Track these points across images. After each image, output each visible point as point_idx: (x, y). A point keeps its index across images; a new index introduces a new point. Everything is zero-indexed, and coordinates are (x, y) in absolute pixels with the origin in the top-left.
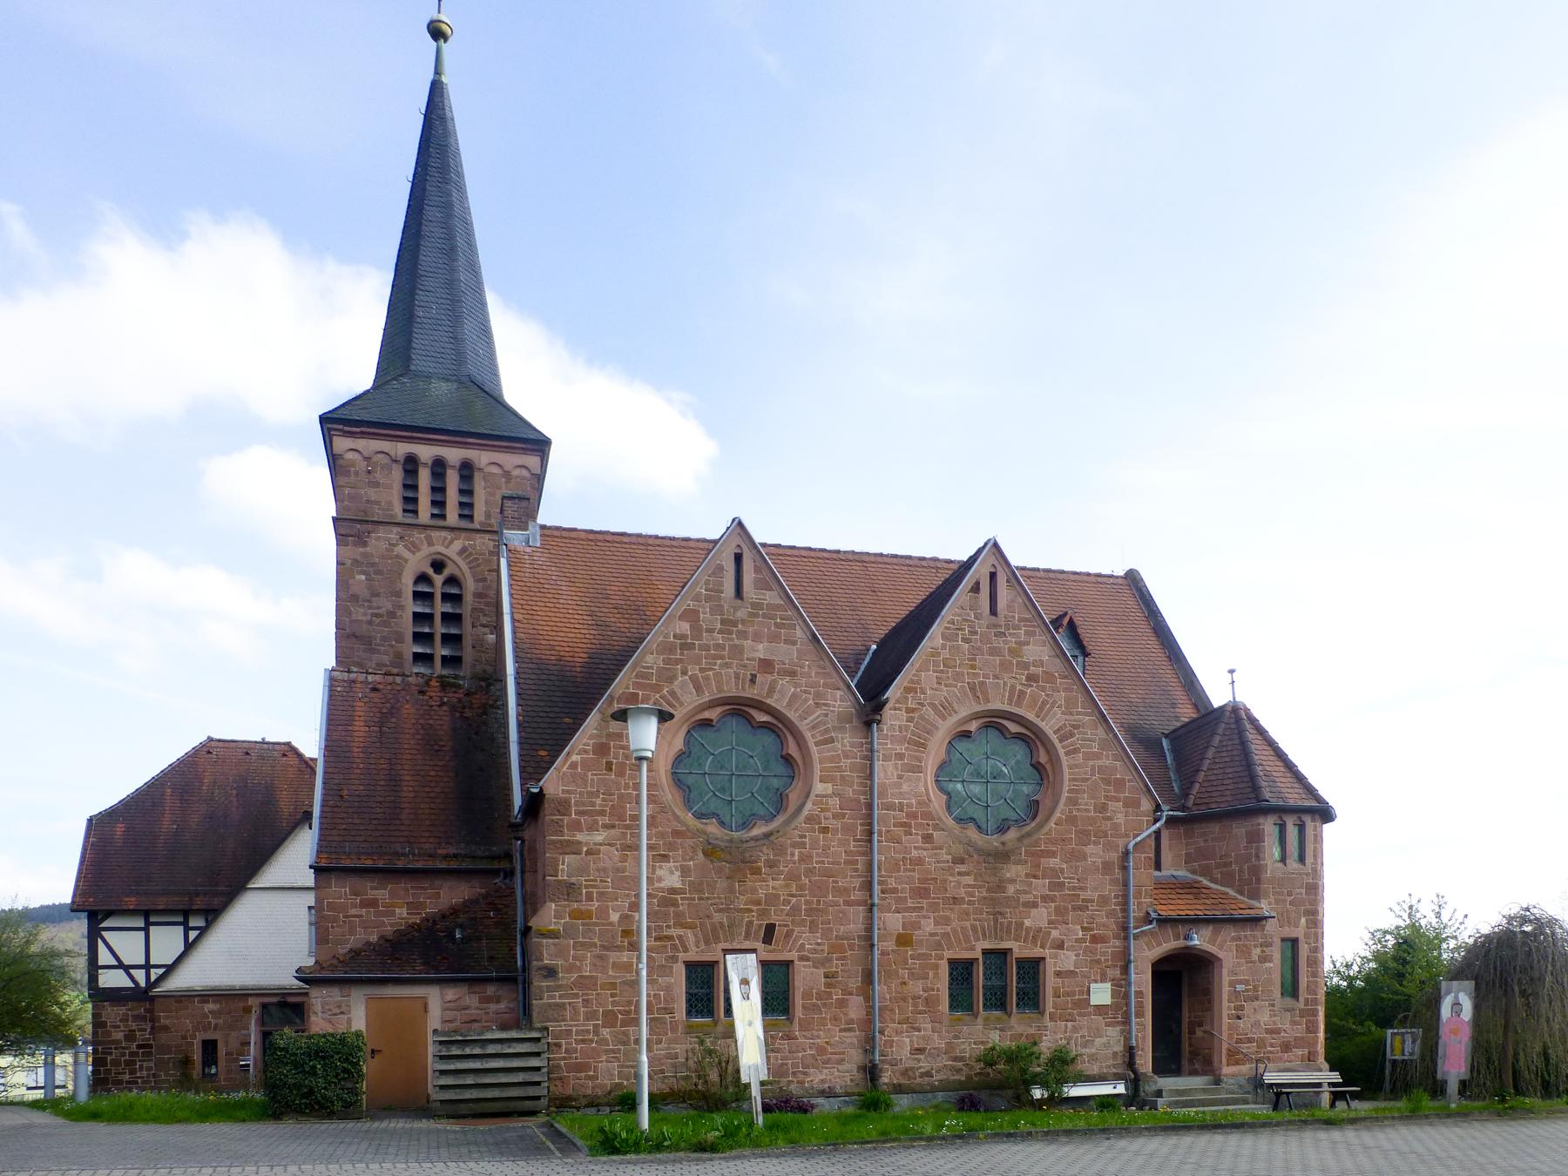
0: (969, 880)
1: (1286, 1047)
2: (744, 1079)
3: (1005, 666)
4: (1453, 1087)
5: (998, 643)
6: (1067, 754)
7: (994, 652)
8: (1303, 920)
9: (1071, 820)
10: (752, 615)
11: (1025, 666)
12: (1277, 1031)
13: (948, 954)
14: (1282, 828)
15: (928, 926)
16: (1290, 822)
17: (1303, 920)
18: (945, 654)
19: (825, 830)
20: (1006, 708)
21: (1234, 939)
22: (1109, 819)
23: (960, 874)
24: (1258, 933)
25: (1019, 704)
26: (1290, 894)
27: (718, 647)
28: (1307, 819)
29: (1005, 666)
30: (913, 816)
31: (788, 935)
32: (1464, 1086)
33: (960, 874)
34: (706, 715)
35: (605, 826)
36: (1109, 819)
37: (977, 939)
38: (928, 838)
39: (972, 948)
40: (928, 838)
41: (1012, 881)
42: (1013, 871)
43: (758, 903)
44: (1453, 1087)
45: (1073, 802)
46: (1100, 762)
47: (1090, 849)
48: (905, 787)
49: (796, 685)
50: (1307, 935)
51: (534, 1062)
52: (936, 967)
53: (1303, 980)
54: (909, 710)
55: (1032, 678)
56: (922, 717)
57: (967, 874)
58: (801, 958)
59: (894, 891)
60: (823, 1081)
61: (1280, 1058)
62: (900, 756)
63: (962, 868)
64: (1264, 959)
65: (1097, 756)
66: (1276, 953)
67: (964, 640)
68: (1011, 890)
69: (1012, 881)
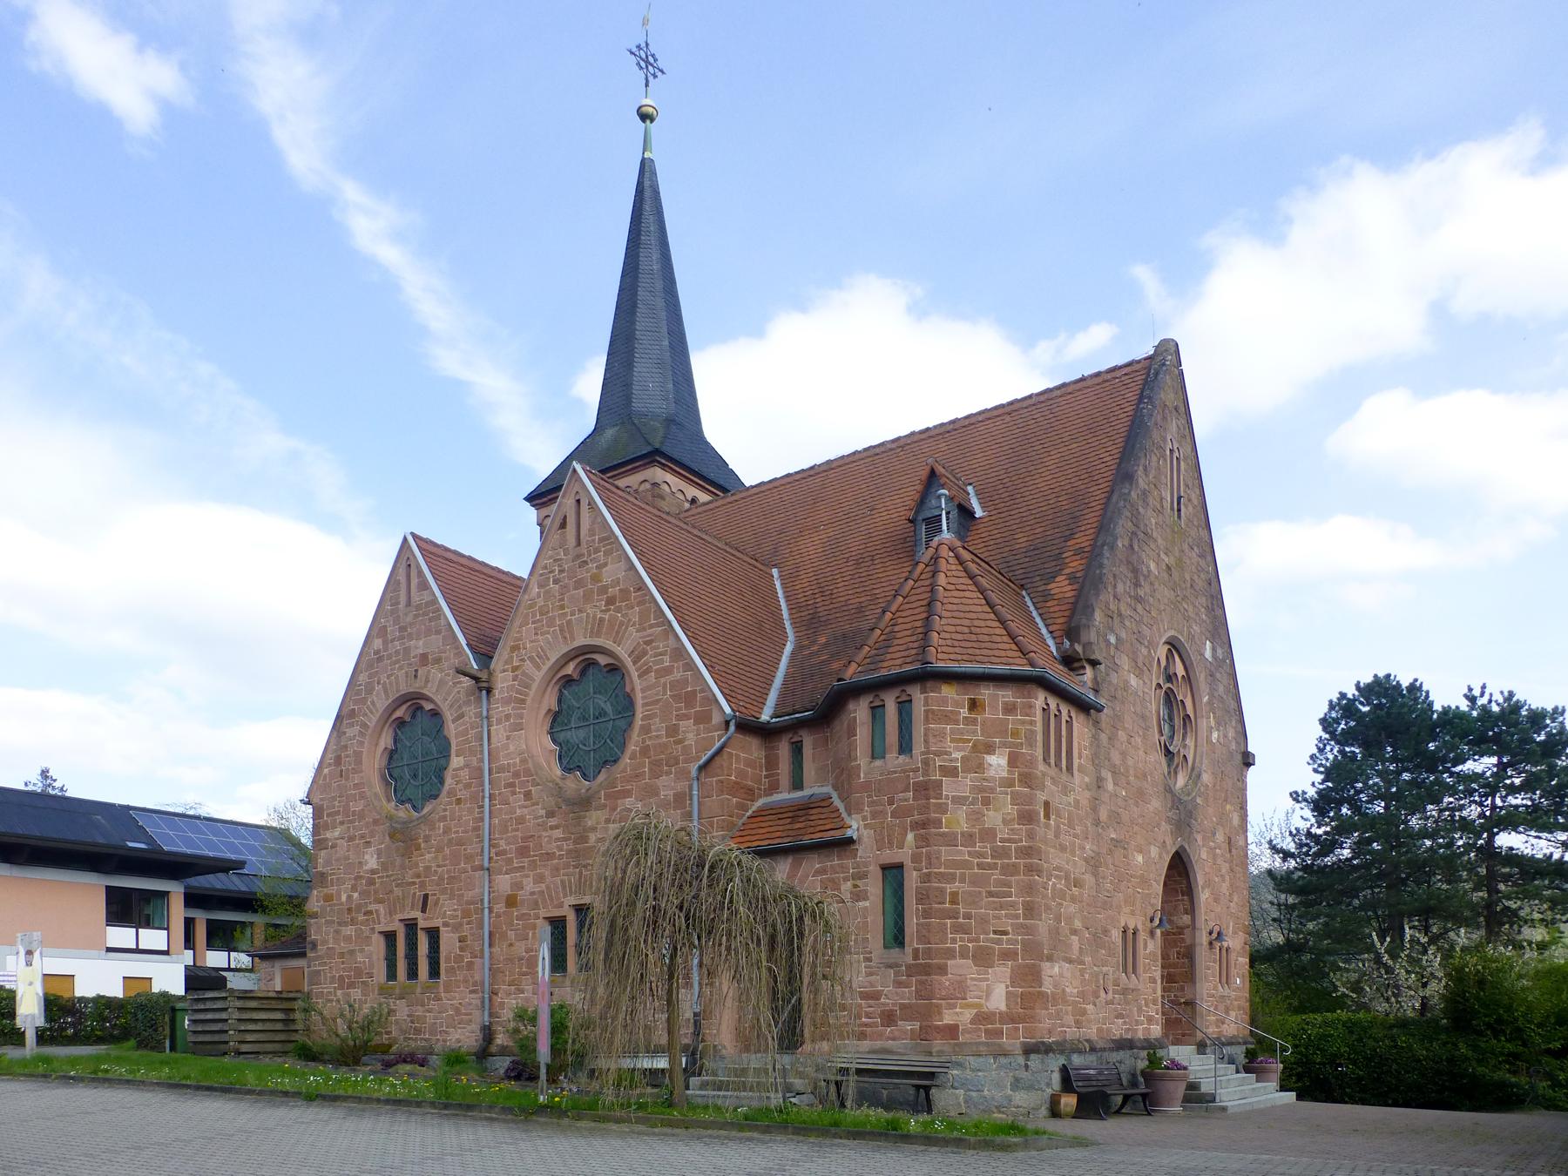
0: (558, 833)
1: (889, 1018)
2: (19, 1022)
3: (587, 597)
4: (30, 1037)
5: (583, 574)
6: (640, 676)
7: (579, 584)
8: (910, 837)
9: (645, 751)
10: (416, 616)
11: (603, 590)
12: (875, 996)
13: (543, 913)
14: (877, 711)
15: (529, 885)
16: (890, 701)
17: (910, 837)
18: (540, 602)
19: (459, 801)
20: (565, 649)
21: (818, 873)
22: (680, 742)
23: (552, 828)
24: (849, 862)
25: (598, 634)
26: (891, 802)
27: (397, 652)
28: (916, 693)
29: (587, 597)
30: (516, 775)
31: (436, 903)
32: (42, 1037)
33: (552, 828)
34: (399, 713)
35: (342, 823)
36: (680, 742)
37: (565, 896)
38: (528, 795)
39: (561, 905)
40: (528, 795)
41: (594, 829)
42: (594, 817)
43: (418, 876)
44: (30, 1037)
45: (646, 729)
46: (670, 678)
47: (663, 781)
48: (512, 748)
49: (442, 671)
50: (916, 858)
51: (224, 1016)
52: (534, 927)
53: (912, 923)
54: (515, 669)
55: (610, 601)
56: (524, 674)
57: (557, 827)
58: (446, 925)
59: (503, 853)
60: (458, 1041)
61: (880, 1036)
62: (508, 717)
63: (553, 822)
64: (858, 896)
65: (668, 671)
66: (874, 886)
67: (555, 582)
68: (593, 837)
69: (594, 829)
